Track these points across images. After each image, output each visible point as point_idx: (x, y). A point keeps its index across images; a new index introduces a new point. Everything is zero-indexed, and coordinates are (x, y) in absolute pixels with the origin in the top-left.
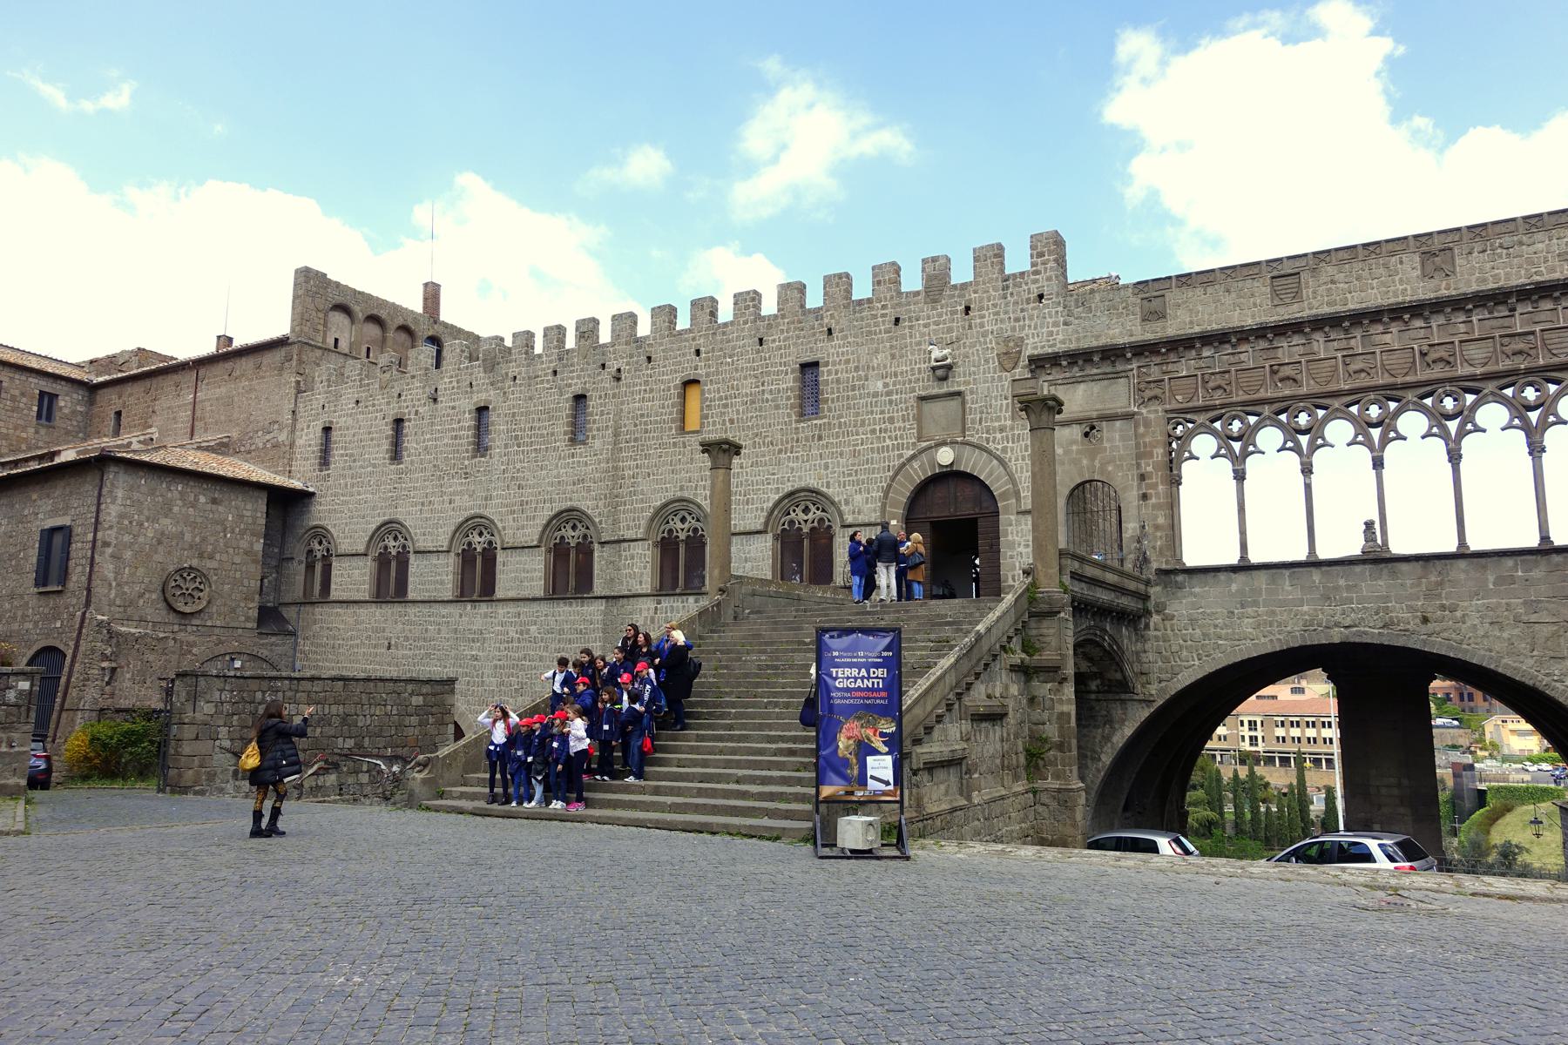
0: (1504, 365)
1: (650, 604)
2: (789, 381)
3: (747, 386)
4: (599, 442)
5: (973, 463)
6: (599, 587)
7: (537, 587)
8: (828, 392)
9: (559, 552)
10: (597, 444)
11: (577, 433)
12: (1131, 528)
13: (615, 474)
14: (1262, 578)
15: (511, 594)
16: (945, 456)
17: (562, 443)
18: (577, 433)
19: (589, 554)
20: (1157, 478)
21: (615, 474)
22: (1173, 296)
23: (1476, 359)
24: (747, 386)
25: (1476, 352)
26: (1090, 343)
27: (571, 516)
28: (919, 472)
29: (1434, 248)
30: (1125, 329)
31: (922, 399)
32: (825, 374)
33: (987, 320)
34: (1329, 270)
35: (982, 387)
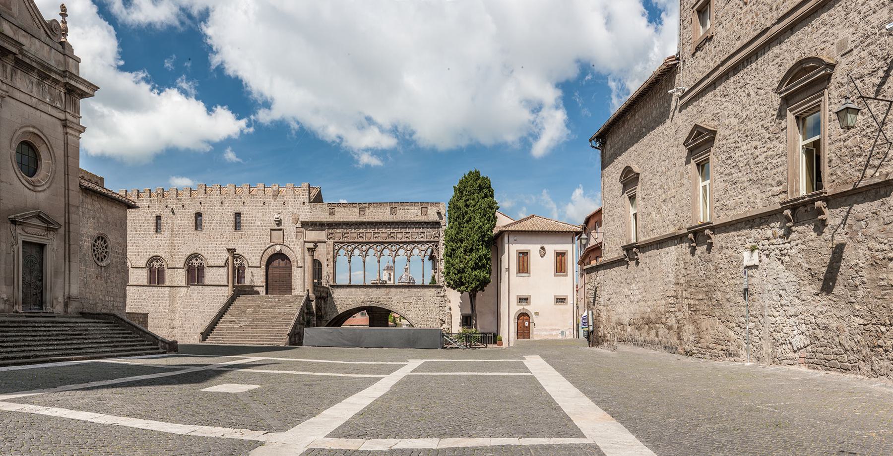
0: (403, 240)
1: (185, 289)
2: (232, 218)
3: (218, 218)
4: (166, 233)
5: (285, 251)
6: (167, 283)
7: (145, 282)
8: (243, 223)
9: (151, 271)
10: (166, 234)
11: (158, 228)
12: (324, 274)
13: (172, 244)
14: (353, 290)
15: (135, 283)
16: (278, 248)
17: (153, 232)
18: (158, 228)
19: (163, 271)
20: (331, 260)
21: (172, 244)
22: (337, 209)
23: (399, 237)
24: (218, 218)
25: (400, 236)
26: (316, 220)
27: (156, 258)
28: (270, 252)
29: (393, 206)
30: (325, 217)
31: (272, 230)
32: (243, 217)
33: (290, 208)
34: (371, 208)
35: (288, 228)
